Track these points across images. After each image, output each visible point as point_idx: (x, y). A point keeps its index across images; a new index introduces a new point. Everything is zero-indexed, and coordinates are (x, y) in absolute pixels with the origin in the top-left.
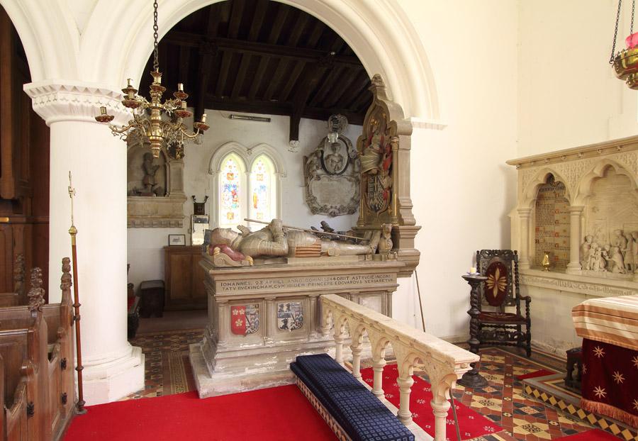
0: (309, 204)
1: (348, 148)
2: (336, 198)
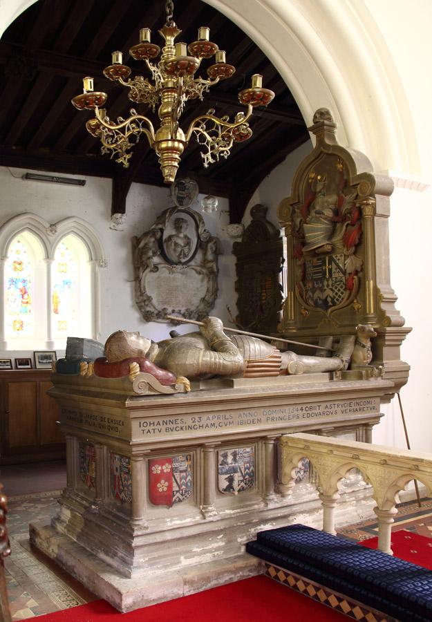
1: (197, 227)
2: (180, 298)
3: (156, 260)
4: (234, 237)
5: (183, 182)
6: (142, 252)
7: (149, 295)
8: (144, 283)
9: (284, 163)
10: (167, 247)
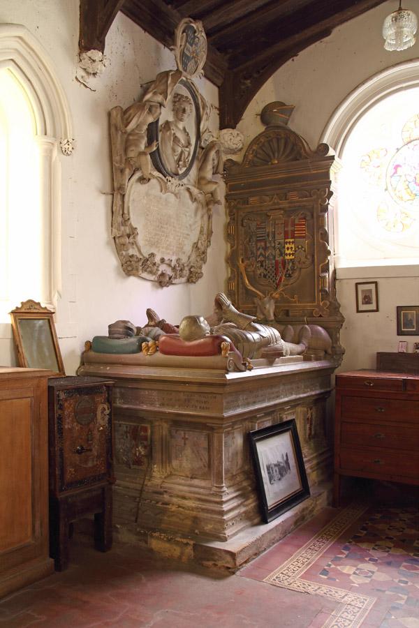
6: (127, 141)
8: (129, 201)
9: (325, 39)
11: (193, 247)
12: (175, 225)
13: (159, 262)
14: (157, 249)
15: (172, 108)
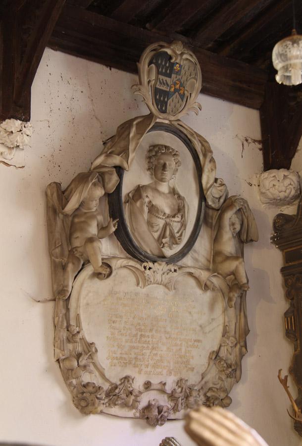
0: (67, 374)
3: (107, 248)
4: (277, 202)
5: (169, 51)
6: (73, 223)
7: (89, 339)
8: (78, 307)
10: (132, 213)
11: (210, 358)
12: (168, 329)
13: (142, 388)
14: (137, 369)
15: (147, 166)
